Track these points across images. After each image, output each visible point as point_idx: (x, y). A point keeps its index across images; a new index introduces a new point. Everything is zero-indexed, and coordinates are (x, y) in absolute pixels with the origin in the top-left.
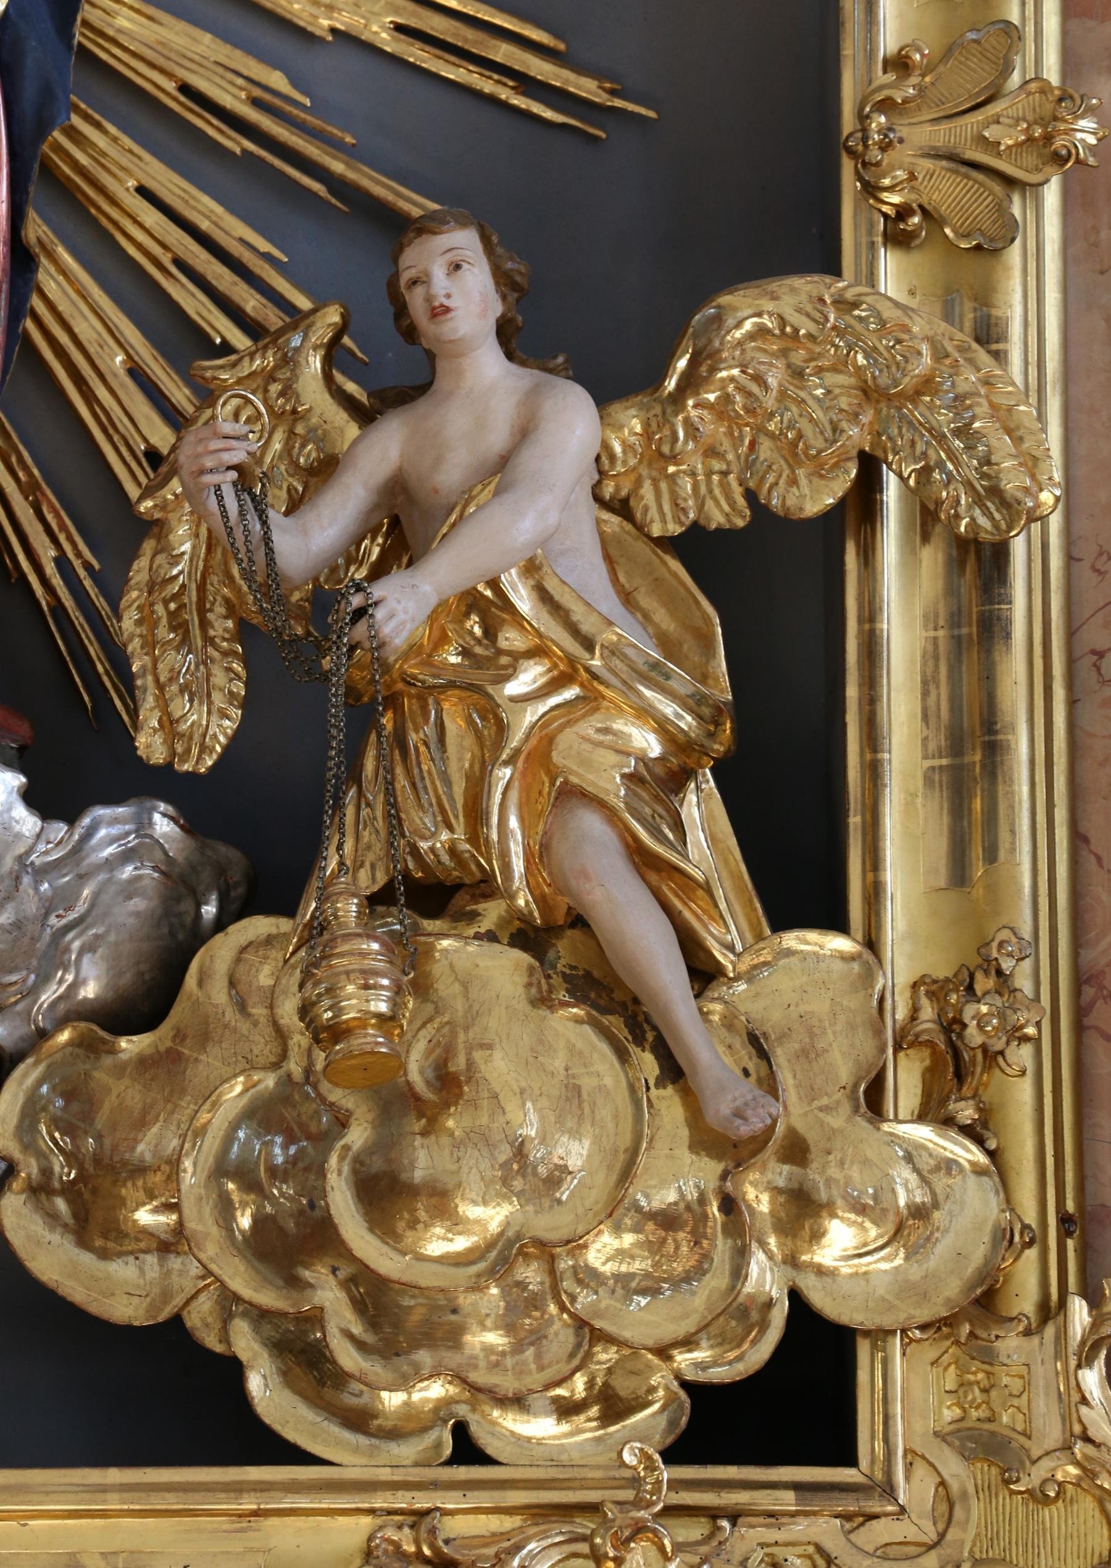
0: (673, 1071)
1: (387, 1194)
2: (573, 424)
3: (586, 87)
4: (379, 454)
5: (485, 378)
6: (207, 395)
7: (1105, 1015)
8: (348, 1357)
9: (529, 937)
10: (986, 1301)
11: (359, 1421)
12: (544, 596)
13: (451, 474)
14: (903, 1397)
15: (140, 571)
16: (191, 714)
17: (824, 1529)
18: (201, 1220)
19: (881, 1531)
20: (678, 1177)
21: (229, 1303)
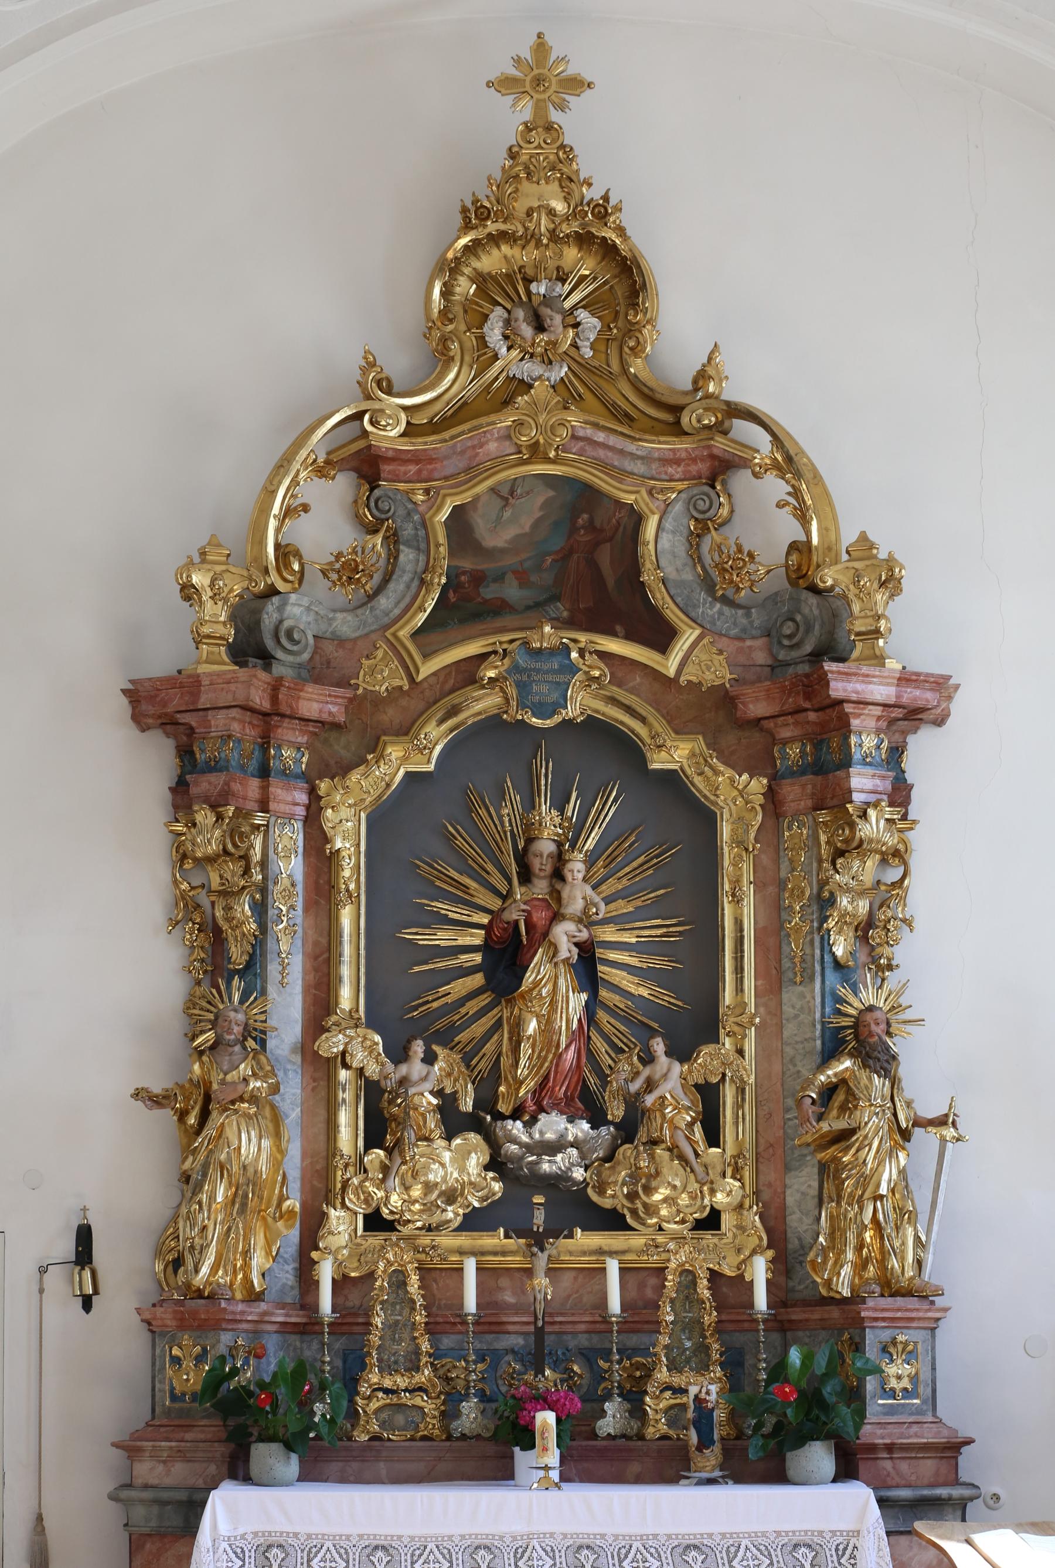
0: (692, 1171)
1: (648, 1190)
2: (677, 1068)
3: (680, 1003)
4: (646, 1072)
5: (663, 1060)
6: (620, 1060)
7: (761, 1160)
8: (642, 1215)
9: (669, 1150)
10: (741, 1206)
11: (644, 1224)
12: (672, 1096)
13: (657, 1076)
14: (727, 1221)
15: (608, 1089)
16: (616, 1111)
17: (716, 1240)
18: (619, 1193)
19: (724, 1241)
20: (694, 1186)
21: (623, 1206)
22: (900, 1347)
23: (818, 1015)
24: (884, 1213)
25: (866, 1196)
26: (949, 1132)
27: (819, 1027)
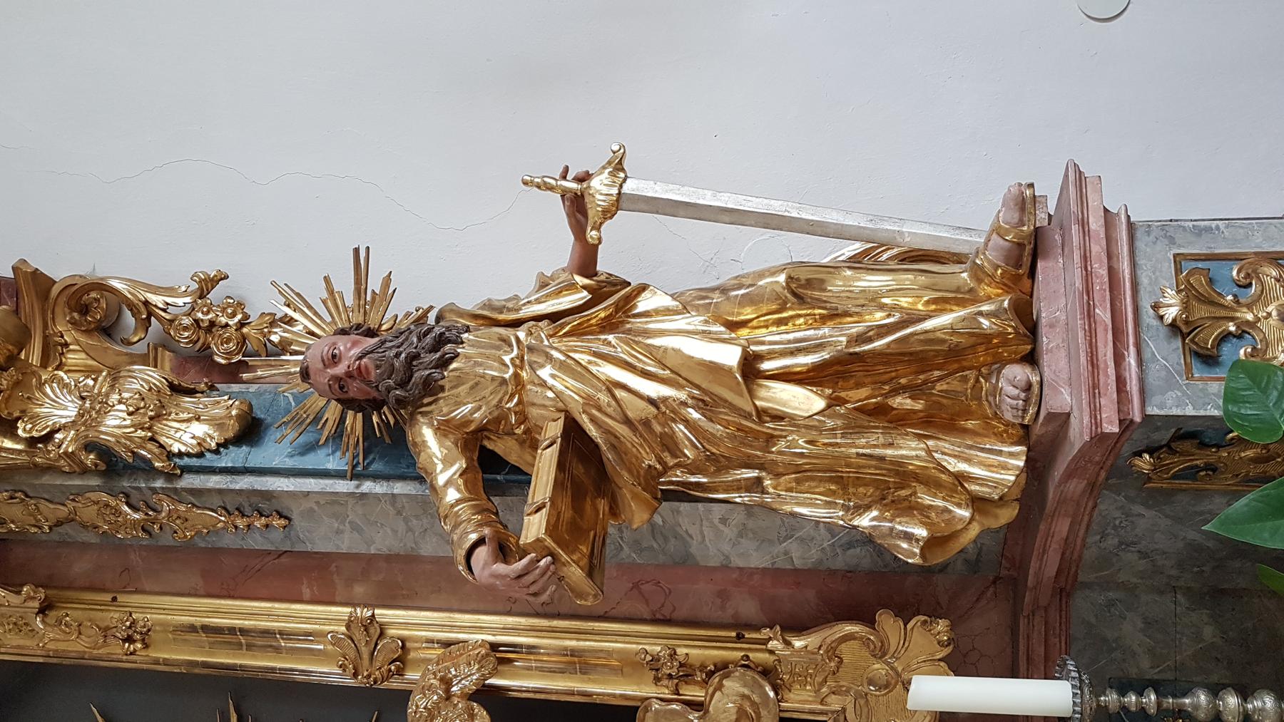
7: (666, 612)
22: (1201, 312)
23: (343, 486)
24: (792, 353)
25: (744, 403)
26: (601, 187)
27: (368, 486)
